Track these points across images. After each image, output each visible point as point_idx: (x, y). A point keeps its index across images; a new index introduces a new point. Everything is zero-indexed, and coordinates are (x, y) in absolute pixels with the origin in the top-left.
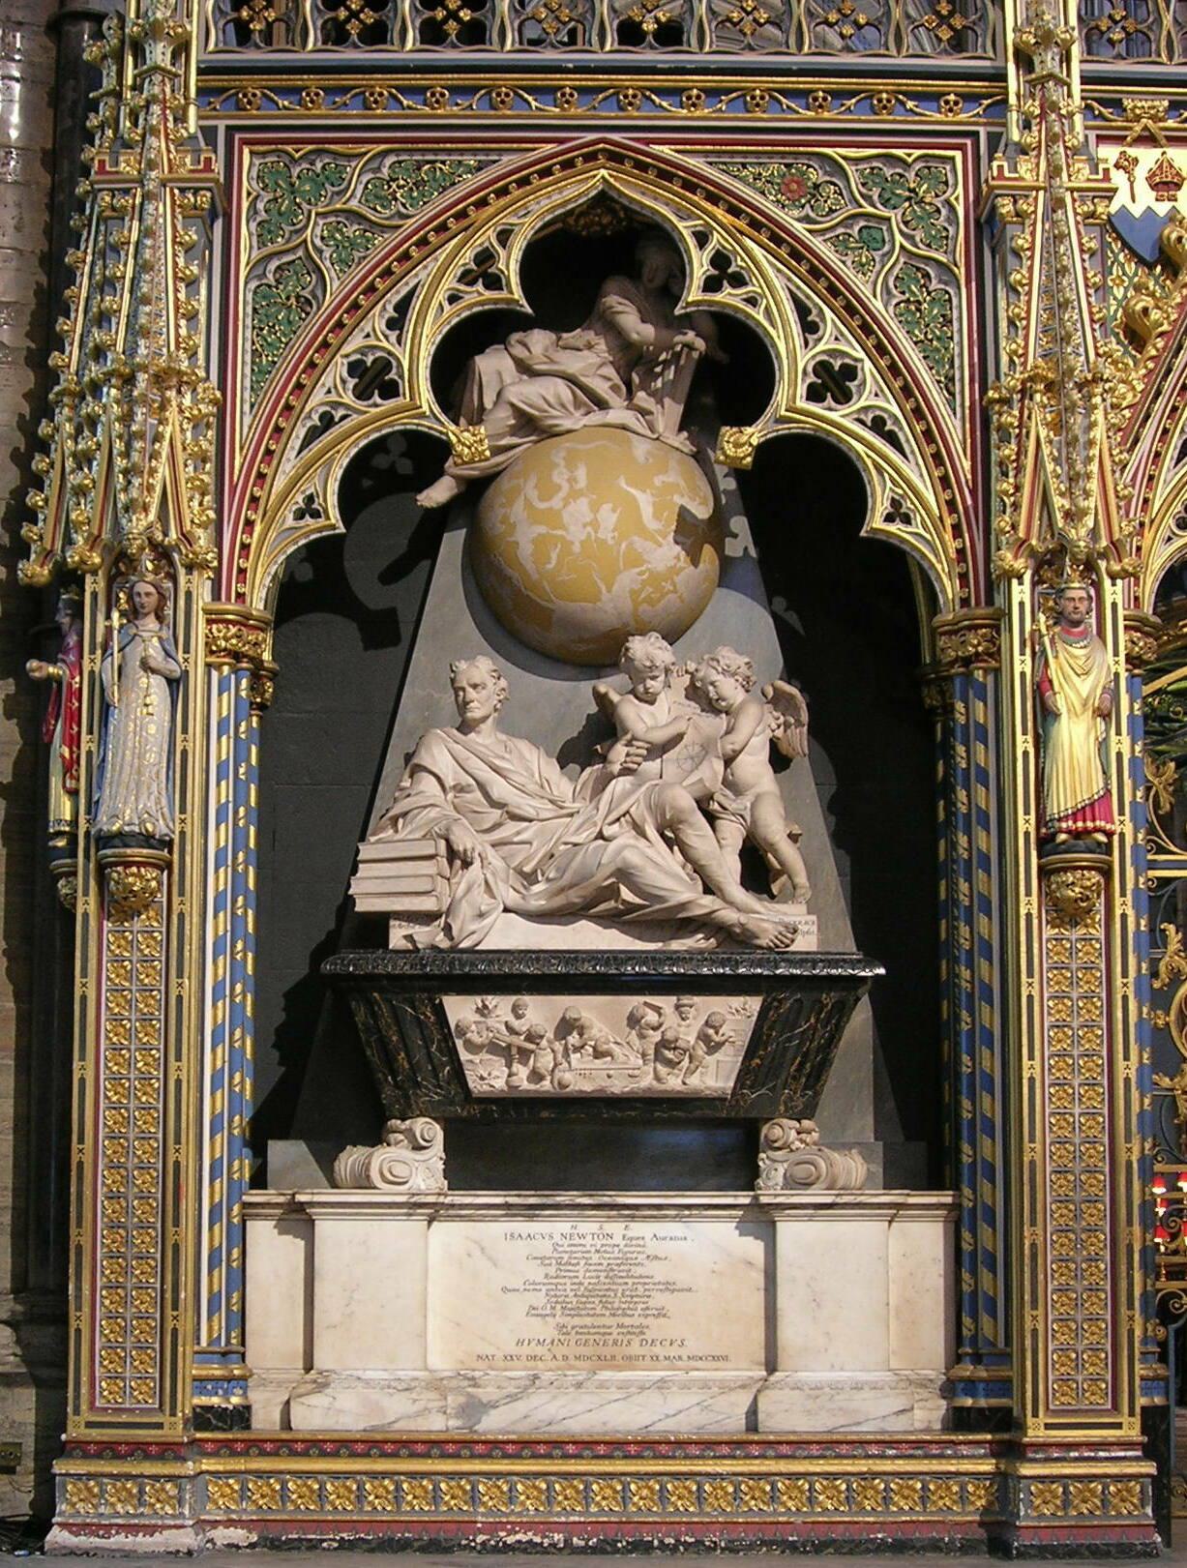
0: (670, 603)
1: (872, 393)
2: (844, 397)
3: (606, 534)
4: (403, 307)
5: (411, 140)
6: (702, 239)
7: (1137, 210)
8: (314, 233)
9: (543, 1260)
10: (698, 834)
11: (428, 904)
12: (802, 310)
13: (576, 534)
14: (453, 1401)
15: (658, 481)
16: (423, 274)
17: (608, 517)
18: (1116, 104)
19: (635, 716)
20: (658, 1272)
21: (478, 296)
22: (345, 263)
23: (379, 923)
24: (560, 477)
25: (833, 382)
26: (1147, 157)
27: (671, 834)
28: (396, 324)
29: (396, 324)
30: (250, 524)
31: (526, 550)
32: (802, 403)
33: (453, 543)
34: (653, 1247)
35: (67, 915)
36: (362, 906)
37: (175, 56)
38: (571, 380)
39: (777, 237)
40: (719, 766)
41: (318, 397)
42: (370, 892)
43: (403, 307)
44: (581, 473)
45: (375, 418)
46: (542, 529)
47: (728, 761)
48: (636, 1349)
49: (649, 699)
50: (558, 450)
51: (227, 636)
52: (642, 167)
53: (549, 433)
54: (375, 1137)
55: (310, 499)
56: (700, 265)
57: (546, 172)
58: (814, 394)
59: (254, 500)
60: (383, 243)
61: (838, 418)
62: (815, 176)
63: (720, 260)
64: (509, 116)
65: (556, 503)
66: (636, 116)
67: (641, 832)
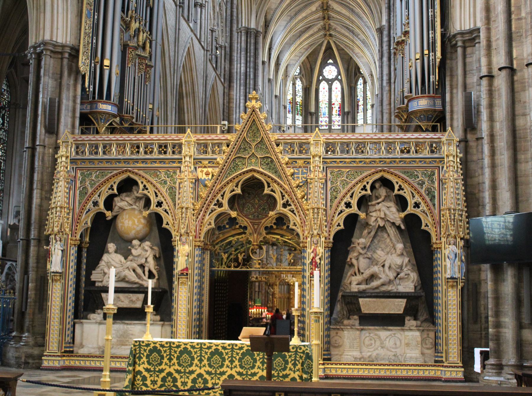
0: (140, 235)
1: (165, 206)
2: (161, 206)
3: (130, 225)
4: (100, 193)
5: (100, 169)
6: (142, 183)
7: (203, 178)
8: (87, 183)
9: (115, 330)
10: (139, 271)
11: (100, 280)
12: (156, 193)
13: (126, 225)
14: (101, 350)
15: (138, 217)
16: (103, 188)
17: (130, 223)
18: (201, 162)
20: (131, 332)
21: (110, 192)
22: (91, 187)
23: (94, 282)
24: (124, 217)
25: (159, 204)
26: (205, 170)
28: (99, 196)
29: (99, 196)
30: (77, 226)
31: (120, 227)
32: (155, 208)
34: (130, 329)
36: (92, 280)
37: (66, 159)
38: (127, 202)
40: (145, 260)
41: (88, 206)
42: (93, 278)
43: (100, 193)
44: (127, 216)
46: (121, 224)
47: (146, 259)
48: (127, 343)
49: (136, 249)
50: (125, 213)
51: (73, 242)
52: (133, 173)
53: (124, 210)
54: (94, 312)
55: (86, 222)
57: (120, 174)
58: (157, 206)
59: (78, 222)
60: (97, 184)
61: (160, 210)
62: (158, 173)
63: (145, 186)
64: (114, 165)
65: (123, 220)
66: (132, 165)
67: (129, 270)
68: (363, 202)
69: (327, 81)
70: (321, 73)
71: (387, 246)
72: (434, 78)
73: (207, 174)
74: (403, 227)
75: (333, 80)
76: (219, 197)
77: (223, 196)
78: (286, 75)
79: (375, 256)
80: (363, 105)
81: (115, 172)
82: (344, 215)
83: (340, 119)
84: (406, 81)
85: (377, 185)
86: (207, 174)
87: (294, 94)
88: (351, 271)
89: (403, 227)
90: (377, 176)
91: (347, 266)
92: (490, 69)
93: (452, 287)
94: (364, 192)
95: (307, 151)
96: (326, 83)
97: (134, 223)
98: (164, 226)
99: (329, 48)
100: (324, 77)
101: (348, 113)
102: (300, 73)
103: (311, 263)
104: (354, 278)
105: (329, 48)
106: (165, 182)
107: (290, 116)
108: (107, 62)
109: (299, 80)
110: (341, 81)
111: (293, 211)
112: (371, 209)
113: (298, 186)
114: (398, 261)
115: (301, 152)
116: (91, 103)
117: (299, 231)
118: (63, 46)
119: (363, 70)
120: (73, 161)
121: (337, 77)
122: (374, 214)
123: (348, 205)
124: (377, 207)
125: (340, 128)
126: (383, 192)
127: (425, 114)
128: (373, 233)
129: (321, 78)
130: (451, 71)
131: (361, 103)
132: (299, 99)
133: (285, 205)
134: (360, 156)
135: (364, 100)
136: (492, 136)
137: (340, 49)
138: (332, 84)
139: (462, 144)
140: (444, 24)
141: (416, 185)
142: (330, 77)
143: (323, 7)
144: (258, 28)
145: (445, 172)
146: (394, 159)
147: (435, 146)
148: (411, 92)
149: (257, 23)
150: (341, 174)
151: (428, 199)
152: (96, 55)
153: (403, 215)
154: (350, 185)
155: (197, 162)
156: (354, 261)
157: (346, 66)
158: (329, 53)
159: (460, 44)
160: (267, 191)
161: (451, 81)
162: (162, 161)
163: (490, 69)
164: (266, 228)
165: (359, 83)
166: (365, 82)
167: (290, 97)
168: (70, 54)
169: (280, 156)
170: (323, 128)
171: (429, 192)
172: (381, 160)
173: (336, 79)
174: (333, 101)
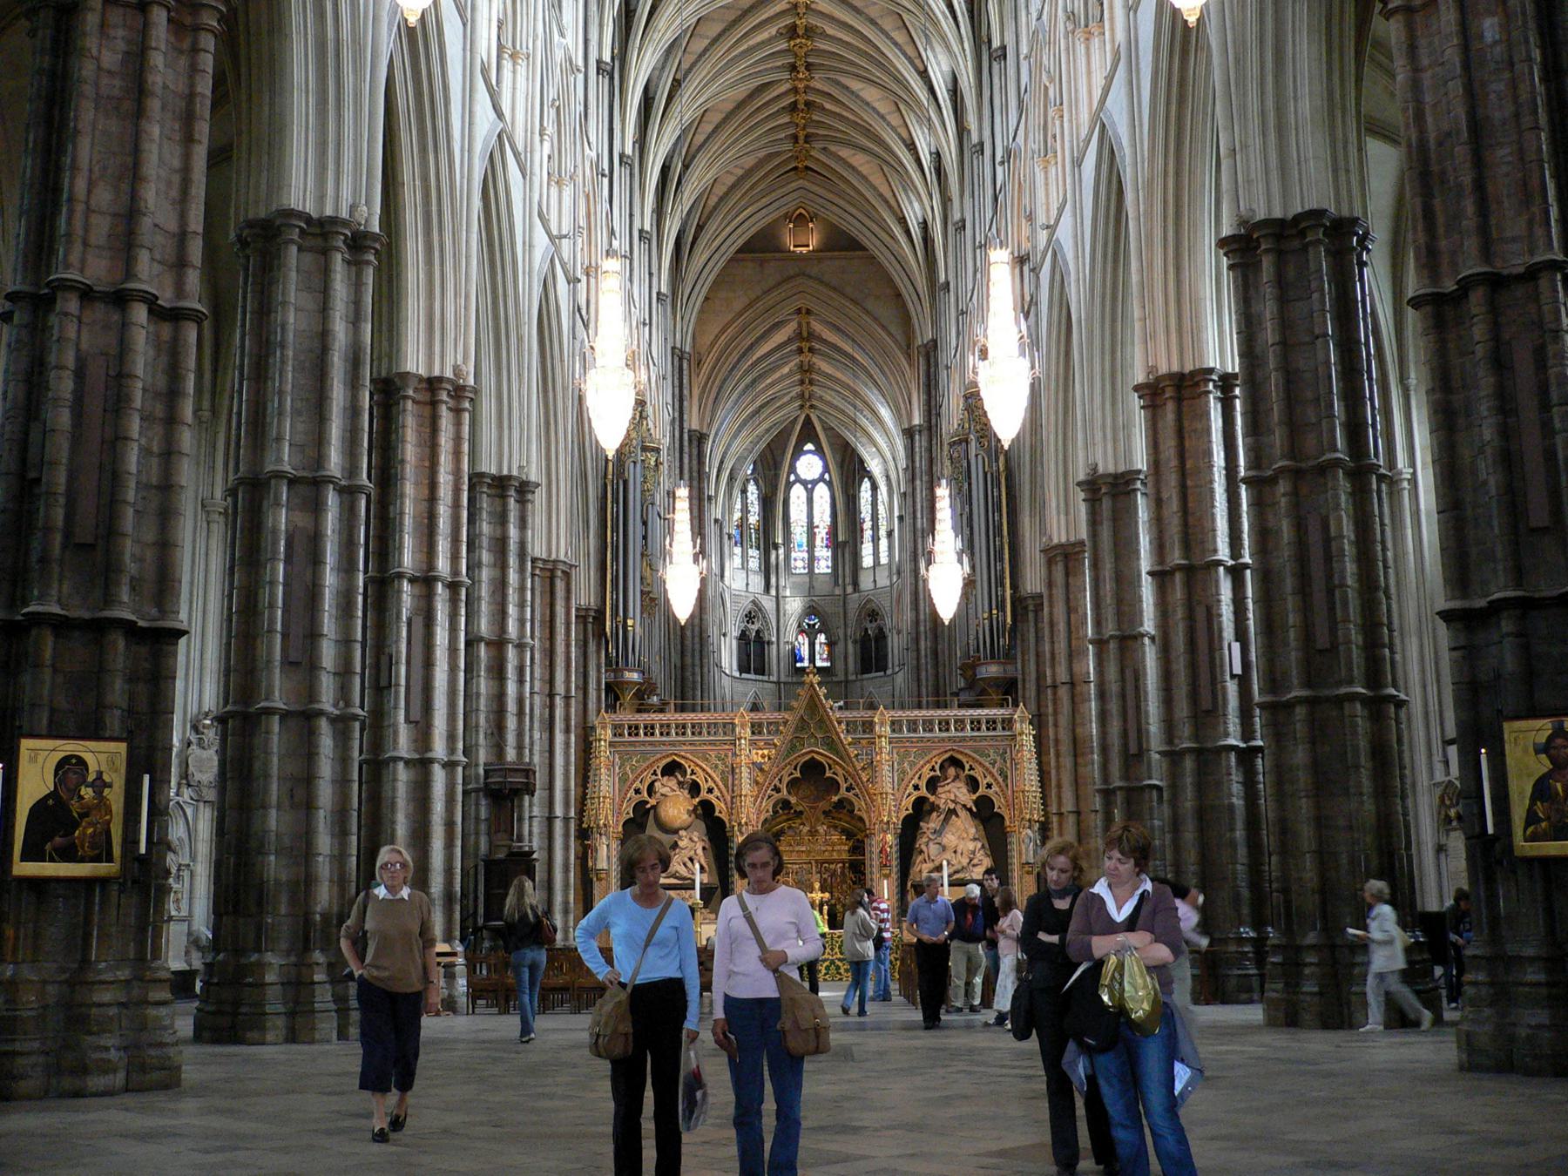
0: (687, 823)
1: (716, 792)
5: (642, 753)
10: (689, 864)
19: (681, 844)
21: (654, 777)
25: (710, 791)
26: (760, 752)
27: (685, 864)
33: (652, 812)
35: (591, 881)
39: (701, 768)
45: (638, 798)
56: (689, 771)
61: (711, 797)
68: (933, 784)
69: (804, 483)
70: (792, 469)
71: (958, 829)
72: (1004, 641)
73: (763, 756)
74: (974, 809)
75: (815, 483)
76: (776, 781)
77: (780, 780)
78: (731, 478)
79: (945, 841)
80: (872, 529)
81: (659, 756)
82: (913, 798)
83: (829, 554)
84: (972, 637)
85: (946, 765)
86: (763, 756)
87: (745, 510)
88: (920, 858)
89: (974, 809)
90: (946, 756)
91: (915, 853)
92: (1054, 680)
93: (1028, 873)
94: (932, 773)
95: (872, 730)
96: (802, 488)
97: (679, 812)
98: (717, 814)
99: (808, 421)
100: (797, 476)
101: (845, 543)
102: (754, 470)
103: (881, 852)
104: (924, 866)
105: (808, 422)
106: (716, 766)
107: (738, 550)
108: (630, 622)
109: (752, 482)
110: (830, 484)
111: (857, 795)
112: (940, 790)
113: (863, 769)
114: (971, 846)
115: (864, 732)
116: (615, 671)
117: (865, 816)
118: (587, 610)
119: (874, 466)
120: (611, 744)
121: (822, 475)
122: (943, 796)
123: (916, 787)
124: (947, 788)
125: (829, 571)
126: (952, 771)
127: (994, 682)
128: (942, 817)
129: (792, 478)
130: (1022, 635)
131: (867, 525)
132: (753, 519)
133: (848, 789)
134: (927, 735)
135: (872, 520)
136: (1057, 741)
137: (828, 429)
138: (813, 489)
139: (1036, 720)
140: (1014, 587)
141: (987, 764)
142: (809, 478)
143: (801, 366)
144: (702, 427)
145: (1018, 751)
146: (964, 739)
147: (1008, 723)
148: (978, 651)
149: (701, 420)
150: (907, 754)
151: (1000, 780)
152: (617, 614)
153: (974, 797)
154: (918, 766)
155: (753, 743)
156: (924, 848)
157: (838, 457)
158: (808, 433)
159: (1031, 607)
160: (828, 774)
161: (1022, 647)
162: (712, 743)
163: (1054, 680)
164: (824, 812)
165: (863, 488)
166: (874, 488)
167: (737, 515)
168: (594, 618)
169: (842, 736)
170: (798, 571)
171: (1002, 772)
172: (950, 739)
173: (821, 479)
174: (816, 521)
